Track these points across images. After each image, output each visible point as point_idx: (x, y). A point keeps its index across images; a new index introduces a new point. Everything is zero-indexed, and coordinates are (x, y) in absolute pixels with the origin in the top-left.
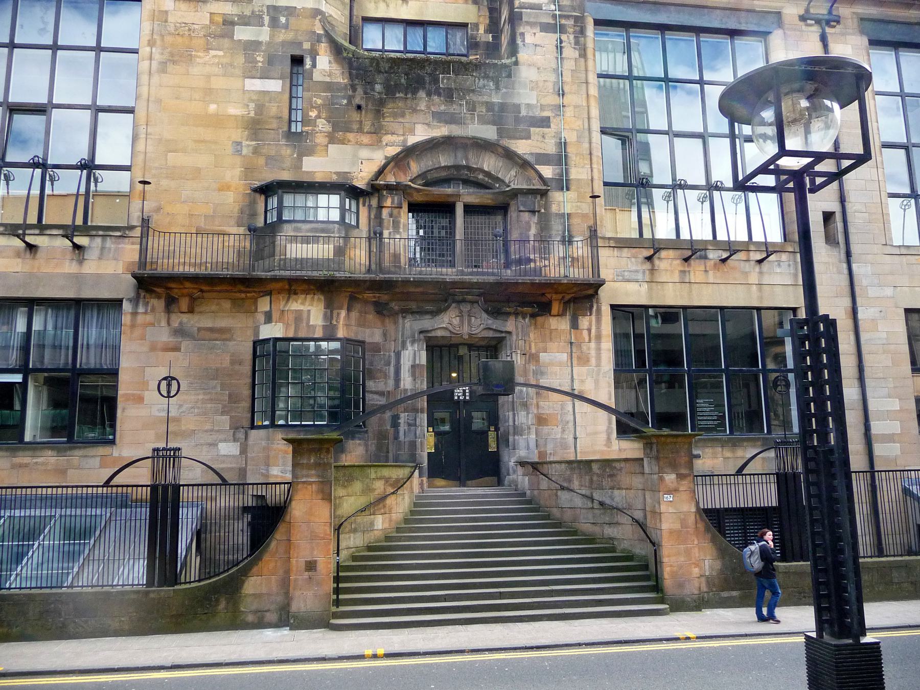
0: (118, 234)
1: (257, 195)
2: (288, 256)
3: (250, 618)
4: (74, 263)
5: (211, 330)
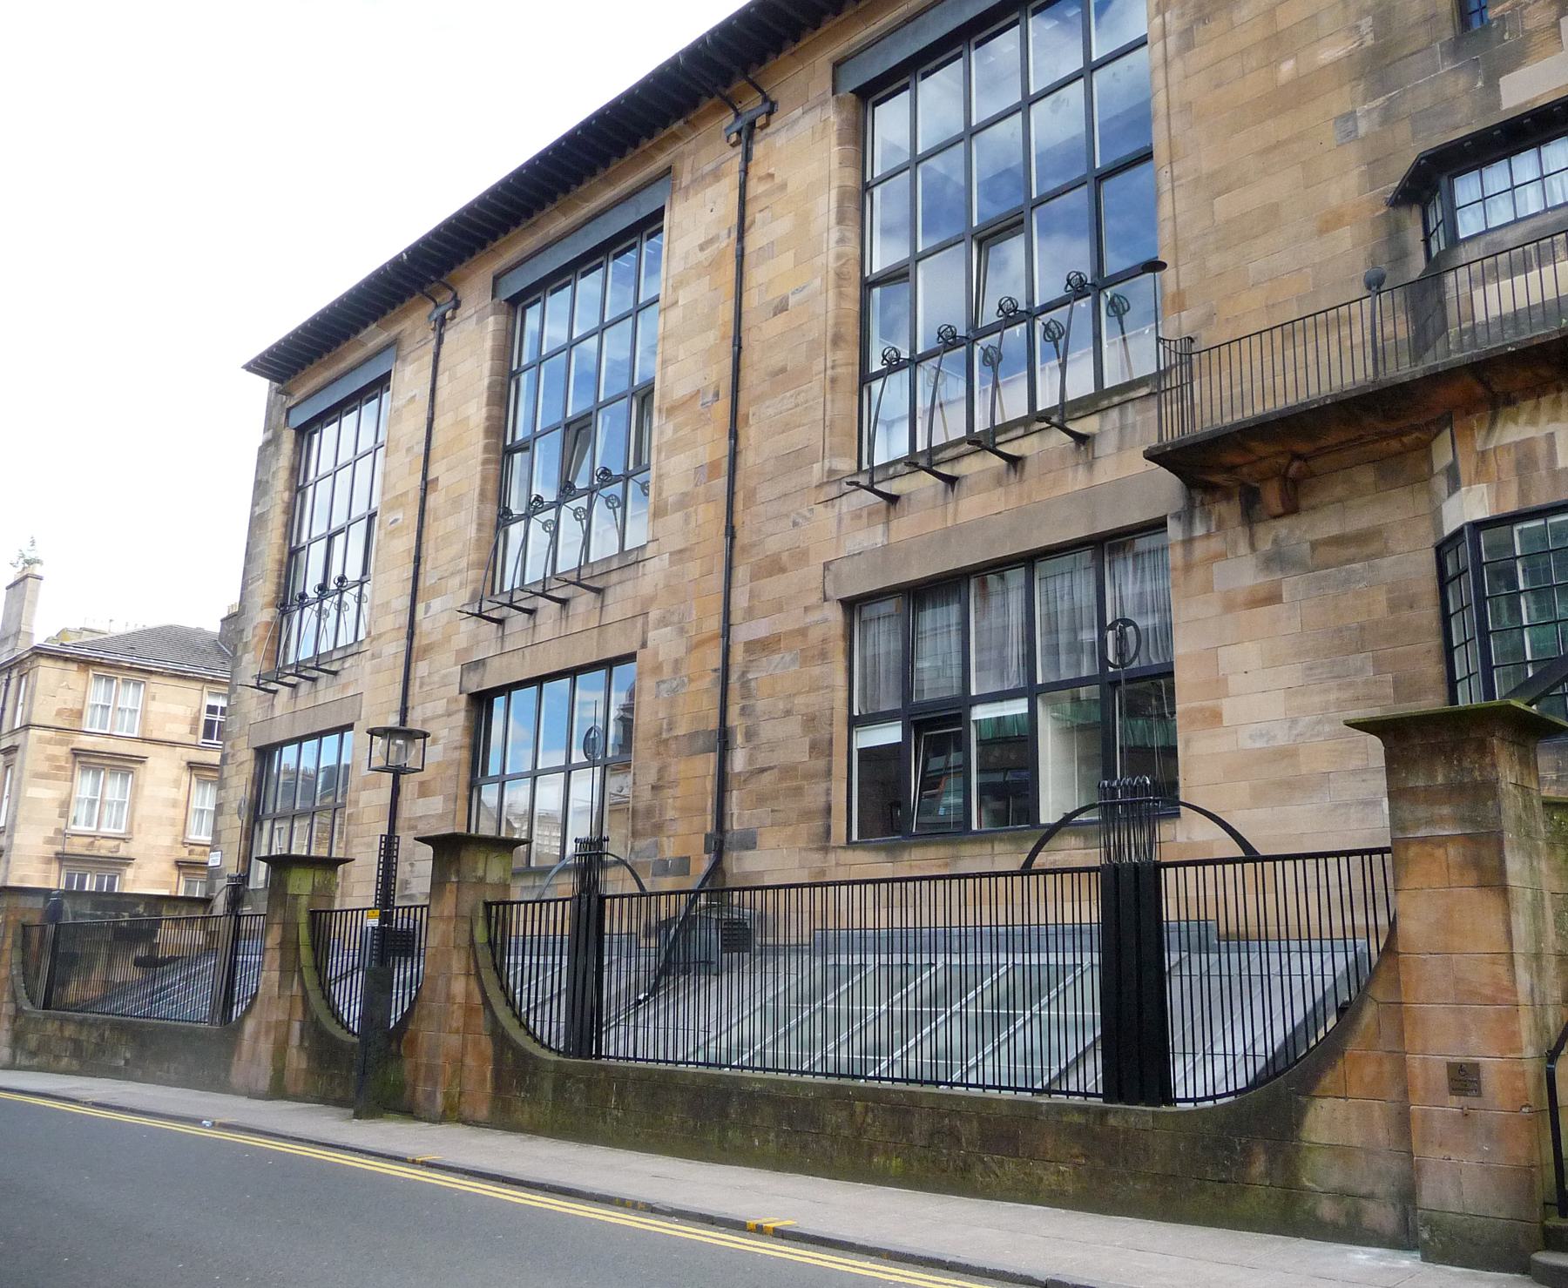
0: (1144, 391)
1: (1403, 212)
2: (1480, 317)
3: (1327, 1210)
4: (1081, 468)
5: (1338, 541)
